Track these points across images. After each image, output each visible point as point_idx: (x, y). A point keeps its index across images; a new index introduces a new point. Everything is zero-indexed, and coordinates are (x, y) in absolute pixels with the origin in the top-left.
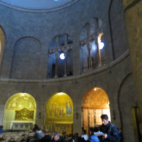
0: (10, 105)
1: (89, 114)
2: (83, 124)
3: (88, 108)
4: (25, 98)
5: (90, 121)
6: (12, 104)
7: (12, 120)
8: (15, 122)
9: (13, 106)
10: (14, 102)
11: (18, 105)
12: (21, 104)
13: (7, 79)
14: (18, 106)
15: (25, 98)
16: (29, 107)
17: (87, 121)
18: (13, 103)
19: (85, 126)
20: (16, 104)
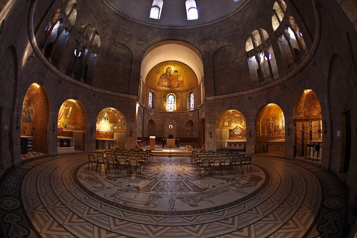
0: (221, 123)
1: (303, 128)
2: (296, 142)
3: (301, 120)
4: (236, 116)
5: (304, 138)
6: (224, 123)
7: (226, 139)
8: (229, 141)
9: (226, 125)
10: (225, 121)
11: (231, 123)
12: (233, 122)
13: (211, 98)
14: (231, 125)
15: (236, 116)
16: (242, 124)
17: (301, 138)
18: (224, 122)
19: (297, 145)
20: (228, 123)
